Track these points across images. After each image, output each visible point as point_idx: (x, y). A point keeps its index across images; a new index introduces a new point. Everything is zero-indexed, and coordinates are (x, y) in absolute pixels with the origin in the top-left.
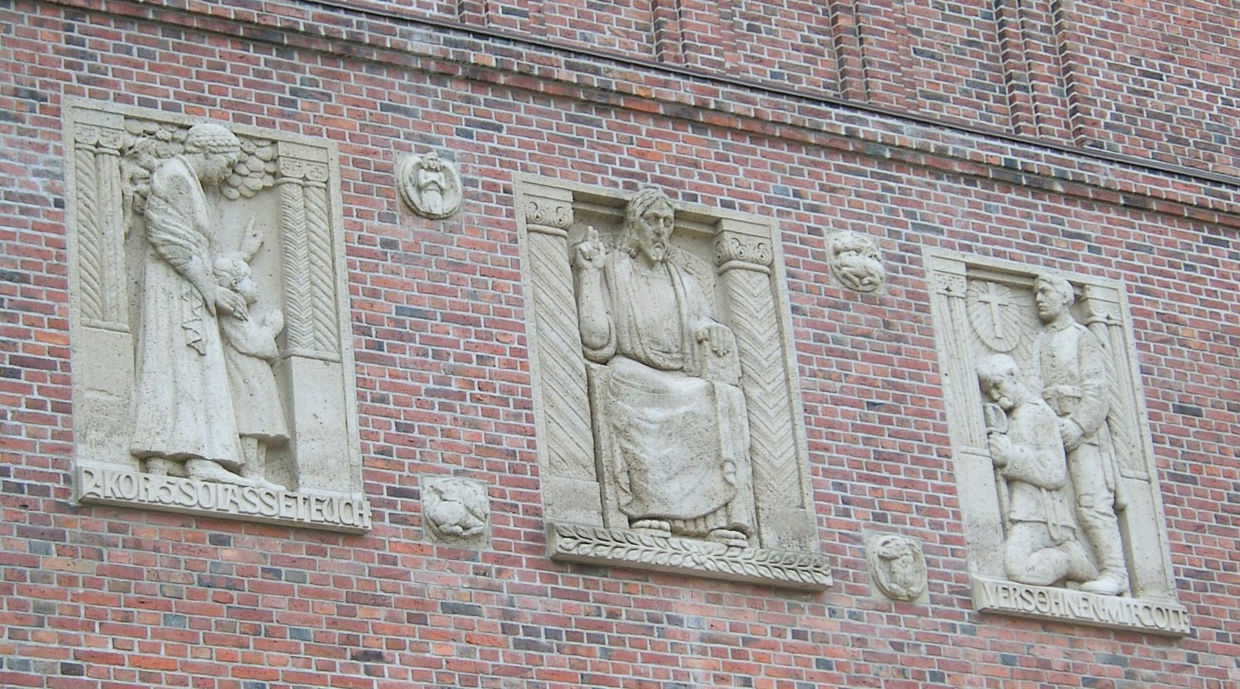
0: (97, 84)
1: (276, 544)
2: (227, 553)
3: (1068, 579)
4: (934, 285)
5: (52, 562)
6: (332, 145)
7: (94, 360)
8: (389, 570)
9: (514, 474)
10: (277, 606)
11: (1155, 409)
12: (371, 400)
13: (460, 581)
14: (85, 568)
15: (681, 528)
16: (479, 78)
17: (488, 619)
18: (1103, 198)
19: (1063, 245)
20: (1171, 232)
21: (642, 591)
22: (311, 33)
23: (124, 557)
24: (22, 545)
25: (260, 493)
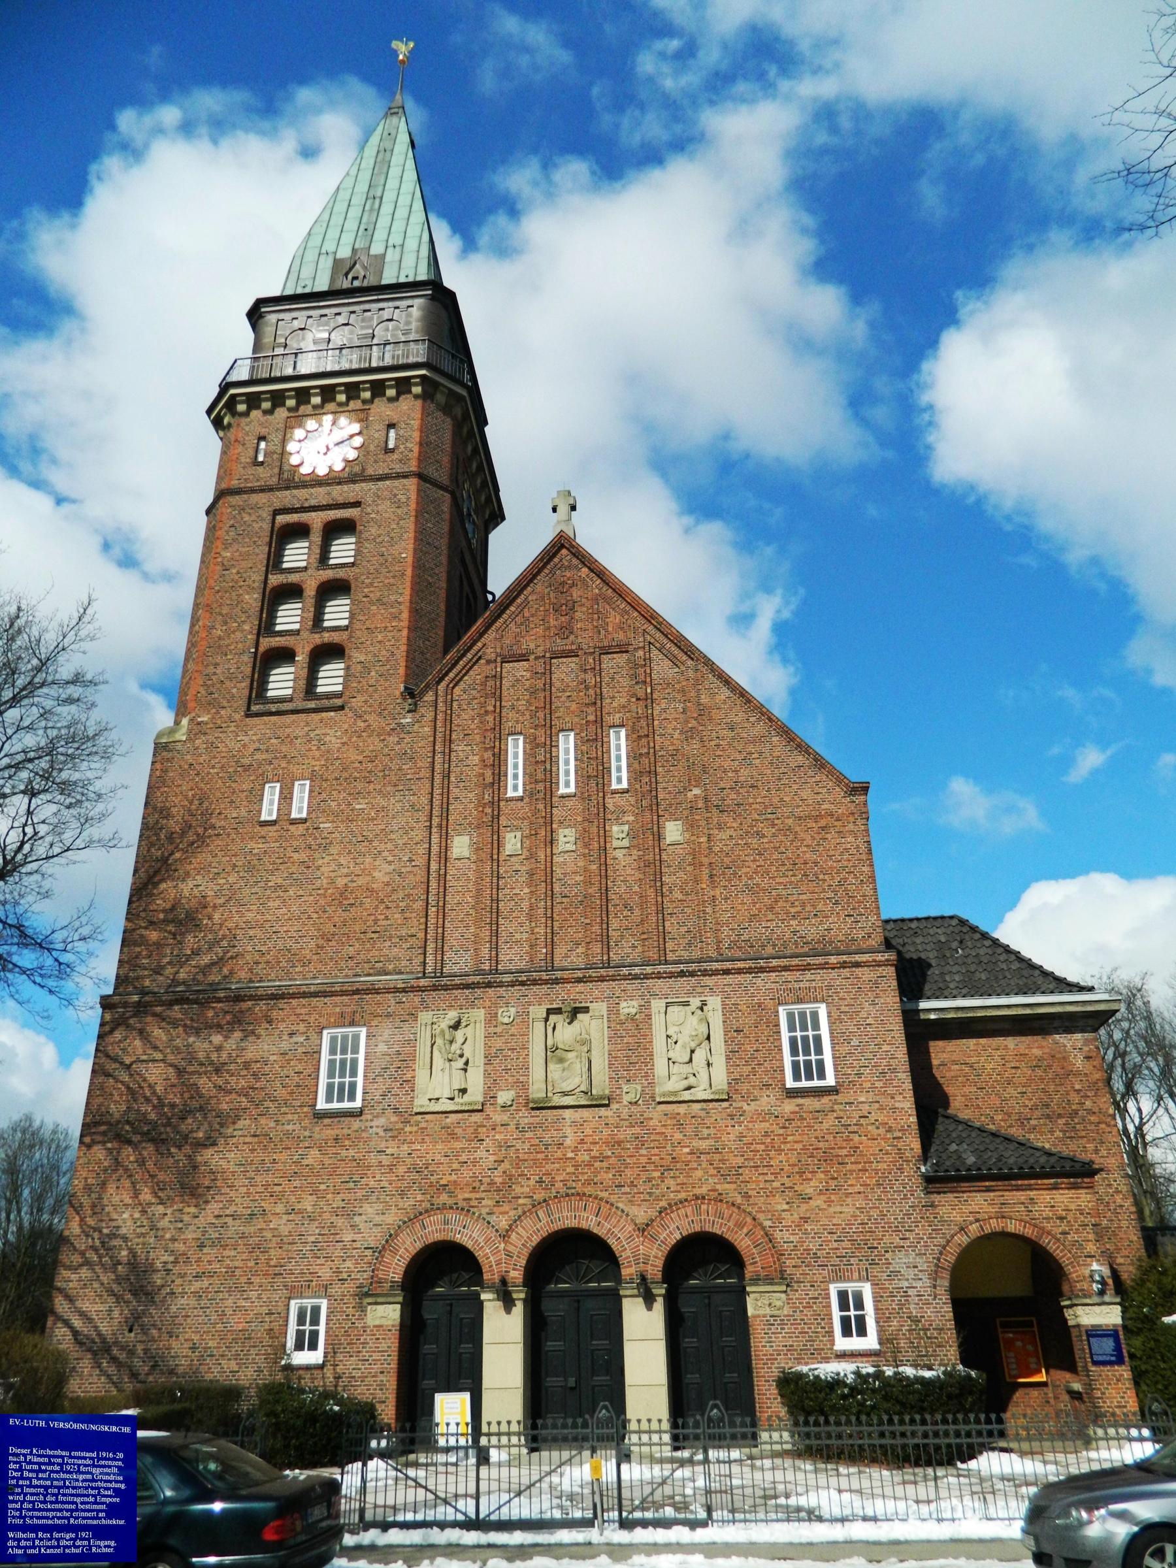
0: (427, 1008)
1: (460, 1116)
2: (448, 1120)
3: (689, 1088)
4: (654, 1010)
5: (408, 1129)
6: (483, 1011)
7: (421, 1075)
8: (488, 1118)
9: (524, 1086)
10: (459, 1131)
11: (726, 1033)
12: (487, 1074)
13: (506, 1118)
14: (415, 1129)
15: (565, 1094)
16: (523, 984)
17: (512, 1126)
18: (715, 973)
19: (699, 990)
20: (739, 977)
21: (555, 1112)
22: (478, 983)
23: (423, 1125)
24: (401, 1126)
25: (461, 1102)
